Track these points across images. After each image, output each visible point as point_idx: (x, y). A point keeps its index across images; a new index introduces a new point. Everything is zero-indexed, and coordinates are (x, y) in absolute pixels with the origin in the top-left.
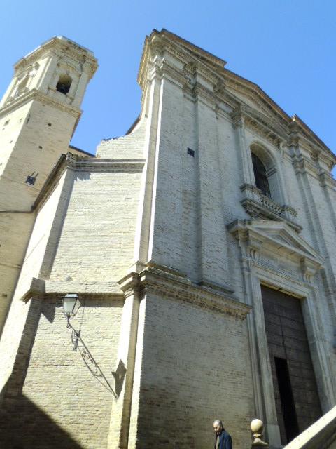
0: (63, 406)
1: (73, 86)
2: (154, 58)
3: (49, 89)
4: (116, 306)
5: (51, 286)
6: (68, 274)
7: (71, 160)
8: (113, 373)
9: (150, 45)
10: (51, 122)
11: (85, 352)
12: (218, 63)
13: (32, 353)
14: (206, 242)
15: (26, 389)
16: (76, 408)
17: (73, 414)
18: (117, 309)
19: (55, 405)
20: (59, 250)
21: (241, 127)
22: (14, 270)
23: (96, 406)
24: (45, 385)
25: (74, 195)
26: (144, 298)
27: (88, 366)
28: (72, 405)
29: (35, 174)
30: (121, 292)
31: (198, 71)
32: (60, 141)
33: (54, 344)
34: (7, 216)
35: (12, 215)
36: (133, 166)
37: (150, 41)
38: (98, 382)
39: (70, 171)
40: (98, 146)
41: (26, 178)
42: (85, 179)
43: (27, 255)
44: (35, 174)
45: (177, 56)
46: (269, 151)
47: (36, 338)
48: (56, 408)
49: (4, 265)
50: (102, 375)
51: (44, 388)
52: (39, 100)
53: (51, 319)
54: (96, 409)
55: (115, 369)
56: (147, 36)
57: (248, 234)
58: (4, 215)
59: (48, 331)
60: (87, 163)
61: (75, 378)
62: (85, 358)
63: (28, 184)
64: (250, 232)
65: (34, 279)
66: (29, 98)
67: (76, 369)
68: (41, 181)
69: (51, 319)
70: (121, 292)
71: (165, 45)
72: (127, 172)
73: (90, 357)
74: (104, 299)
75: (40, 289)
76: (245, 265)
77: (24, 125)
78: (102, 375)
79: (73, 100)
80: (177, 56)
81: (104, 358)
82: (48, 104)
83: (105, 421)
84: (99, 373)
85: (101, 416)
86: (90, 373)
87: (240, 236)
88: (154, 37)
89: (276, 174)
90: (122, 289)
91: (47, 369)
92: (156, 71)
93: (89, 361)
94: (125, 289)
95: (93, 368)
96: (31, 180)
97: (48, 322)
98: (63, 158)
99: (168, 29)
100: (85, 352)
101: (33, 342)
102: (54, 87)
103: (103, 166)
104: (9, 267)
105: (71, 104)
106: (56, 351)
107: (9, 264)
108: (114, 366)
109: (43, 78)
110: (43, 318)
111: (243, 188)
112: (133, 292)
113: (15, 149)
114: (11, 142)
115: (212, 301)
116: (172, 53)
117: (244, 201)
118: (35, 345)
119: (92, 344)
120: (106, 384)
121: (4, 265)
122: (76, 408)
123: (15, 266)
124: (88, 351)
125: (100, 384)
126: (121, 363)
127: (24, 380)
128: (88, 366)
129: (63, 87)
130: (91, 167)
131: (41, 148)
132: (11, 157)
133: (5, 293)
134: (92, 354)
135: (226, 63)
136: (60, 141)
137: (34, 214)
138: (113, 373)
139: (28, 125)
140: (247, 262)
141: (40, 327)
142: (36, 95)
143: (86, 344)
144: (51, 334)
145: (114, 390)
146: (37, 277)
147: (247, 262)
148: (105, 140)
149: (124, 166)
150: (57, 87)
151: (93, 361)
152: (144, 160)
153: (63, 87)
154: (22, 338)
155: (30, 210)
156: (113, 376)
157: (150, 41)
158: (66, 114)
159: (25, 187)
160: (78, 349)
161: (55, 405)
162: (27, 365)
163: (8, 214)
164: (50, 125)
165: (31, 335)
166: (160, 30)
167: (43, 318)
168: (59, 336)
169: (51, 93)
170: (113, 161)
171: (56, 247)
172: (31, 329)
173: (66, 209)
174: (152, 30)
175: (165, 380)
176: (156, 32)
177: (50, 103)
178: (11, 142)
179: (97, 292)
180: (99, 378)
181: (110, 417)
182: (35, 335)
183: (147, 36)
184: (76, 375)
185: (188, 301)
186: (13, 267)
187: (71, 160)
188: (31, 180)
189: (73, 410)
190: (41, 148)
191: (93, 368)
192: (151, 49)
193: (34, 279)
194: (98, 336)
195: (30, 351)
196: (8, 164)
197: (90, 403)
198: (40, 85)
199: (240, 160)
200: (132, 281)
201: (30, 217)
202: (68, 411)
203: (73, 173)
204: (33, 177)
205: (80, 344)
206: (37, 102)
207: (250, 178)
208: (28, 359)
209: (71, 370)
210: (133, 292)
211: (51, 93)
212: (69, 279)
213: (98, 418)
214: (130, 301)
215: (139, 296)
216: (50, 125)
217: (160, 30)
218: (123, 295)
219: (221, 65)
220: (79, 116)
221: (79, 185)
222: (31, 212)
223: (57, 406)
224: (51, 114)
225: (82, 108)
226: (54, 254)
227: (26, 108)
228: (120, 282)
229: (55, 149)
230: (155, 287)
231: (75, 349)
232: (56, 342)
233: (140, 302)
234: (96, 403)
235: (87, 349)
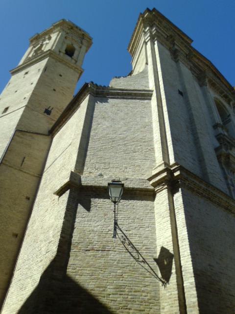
0: (109, 291)
1: (76, 53)
2: (146, 29)
3: (60, 52)
4: (147, 200)
5: (88, 179)
6: (99, 172)
7: (93, 88)
8: (155, 260)
9: (143, 20)
10: (62, 74)
11: (125, 239)
12: (187, 40)
13: (73, 238)
14: (206, 157)
15: (70, 271)
16: (124, 293)
17: (121, 299)
18: (148, 202)
19: (101, 289)
20: (88, 153)
21: (206, 85)
22: (35, 178)
23: (143, 291)
24: (89, 269)
25: (96, 113)
26: (178, 191)
27: (130, 253)
28: (119, 289)
29: (51, 108)
30: (152, 188)
31: (175, 42)
32: (69, 88)
33: (93, 231)
34: (29, 136)
35: (35, 135)
36: (143, 95)
37: (143, 17)
38: (142, 268)
39: (91, 96)
40: (111, 81)
41: (44, 110)
42: (104, 102)
43: (47, 165)
44: (51, 108)
45: (162, 29)
46: (224, 106)
47: (76, 225)
48: (103, 292)
49: (28, 173)
50: (144, 261)
51: (88, 272)
52: (53, 58)
53: (88, 208)
54: (144, 294)
55: (157, 255)
56: (141, 14)
57: (229, 158)
58: (28, 134)
59: (86, 219)
60: (105, 91)
61: (117, 263)
62: (126, 245)
63: (46, 114)
64: (230, 156)
65: (72, 172)
66: (44, 56)
67: (118, 255)
68: (56, 115)
69: (88, 208)
70: (152, 188)
71: (154, 20)
72: (138, 99)
73: (130, 243)
74: (135, 194)
75: (77, 182)
76: (230, 182)
77: (42, 73)
78: (144, 261)
79: (76, 62)
80: (162, 29)
81: (143, 246)
82: (59, 61)
83: (156, 307)
84: (141, 259)
85: (150, 301)
86: (132, 259)
87: (223, 159)
88: (147, 14)
89: (231, 122)
90: (153, 185)
91: (90, 253)
92: (150, 36)
93: (129, 248)
94: (156, 184)
95: (135, 254)
96: (48, 112)
97: (86, 211)
98: (86, 85)
99: (158, 9)
100: (125, 239)
101: (73, 228)
102: (63, 51)
103: (118, 94)
104: (32, 175)
105: (75, 64)
106: (96, 237)
107: (31, 173)
108: (155, 253)
109: (55, 45)
110: (80, 208)
111: (215, 126)
112: (166, 186)
113: (36, 88)
114: (32, 84)
115: (226, 201)
116: (159, 26)
117: (218, 135)
118: (75, 231)
119: (130, 232)
120: (150, 270)
121: (28, 173)
122: (124, 293)
123: (36, 175)
124: (128, 239)
125: (143, 270)
126: (163, 250)
127: (68, 263)
128: (129, 252)
129: (70, 52)
130: (108, 94)
131: (54, 90)
132: (33, 93)
133: (28, 196)
134: (132, 241)
135: (192, 41)
136: (69, 88)
137: (50, 137)
138: (155, 260)
139: (46, 73)
140: (231, 180)
141: (78, 215)
142: (50, 53)
143: (125, 232)
144: (93, 221)
145: (160, 275)
146: (73, 171)
147: (231, 180)
148: (116, 77)
149: (135, 94)
150: (66, 50)
151: (133, 247)
152: (152, 91)
153: (70, 52)
154: (64, 223)
155: (47, 133)
156: (155, 263)
157: (143, 17)
158: (72, 71)
159: (43, 116)
160: (117, 236)
161: (101, 289)
162: (69, 249)
163: (31, 134)
164: (61, 76)
165: (71, 222)
166: (151, 9)
167: (80, 208)
168: (97, 224)
169: (62, 54)
170: (126, 90)
171: (86, 150)
172: (71, 216)
173: (91, 123)
174: (145, 9)
175: (208, 267)
176: (148, 10)
177: (61, 61)
178: (32, 84)
179: (130, 186)
180: (142, 264)
181: (159, 303)
182: (74, 222)
183: (141, 14)
184: (119, 260)
185: (209, 199)
186: (34, 176)
187: (93, 88)
188: (48, 112)
189: (120, 295)
190: (54, 90)
191: (135, 254)
192: (144, 23)
193: (72, 172)
194: (135, 225)
195: (71, 236)
196: (30, 98)
197: (138, 289)
198: (54, 48)
199: (209, 107)
200: (166, 176)
201: (47, 139)
202: (116, 296)
203: (93, 97)
204: (49, 110)
205: (118, 231)
206: (52, 60)
207: (218, 120)
208: (70, 243)
209: (112, 255)
210: (166, 186)
211: (62, 54)
212: (101, 175)
213: (147, 304)
214: (163, 196)
215: (172, 192)
216: (61, 76)
217: (151, 9)
218: (153, 191)
219: (190, 42)
220: (82, 72)
221: (99, 106)
222: (48, 135)
223: (104, 290)
224: (61, 68)
225: (83, 67)
226: (85, 156)
227: (44, 62)
228: (150, 179)
229: (65, 93)
230: (187, 183)
231: (114, 236)
232: (95, 229)
233: (173, 196)
234: (143, 289)
235: (125, 236)
